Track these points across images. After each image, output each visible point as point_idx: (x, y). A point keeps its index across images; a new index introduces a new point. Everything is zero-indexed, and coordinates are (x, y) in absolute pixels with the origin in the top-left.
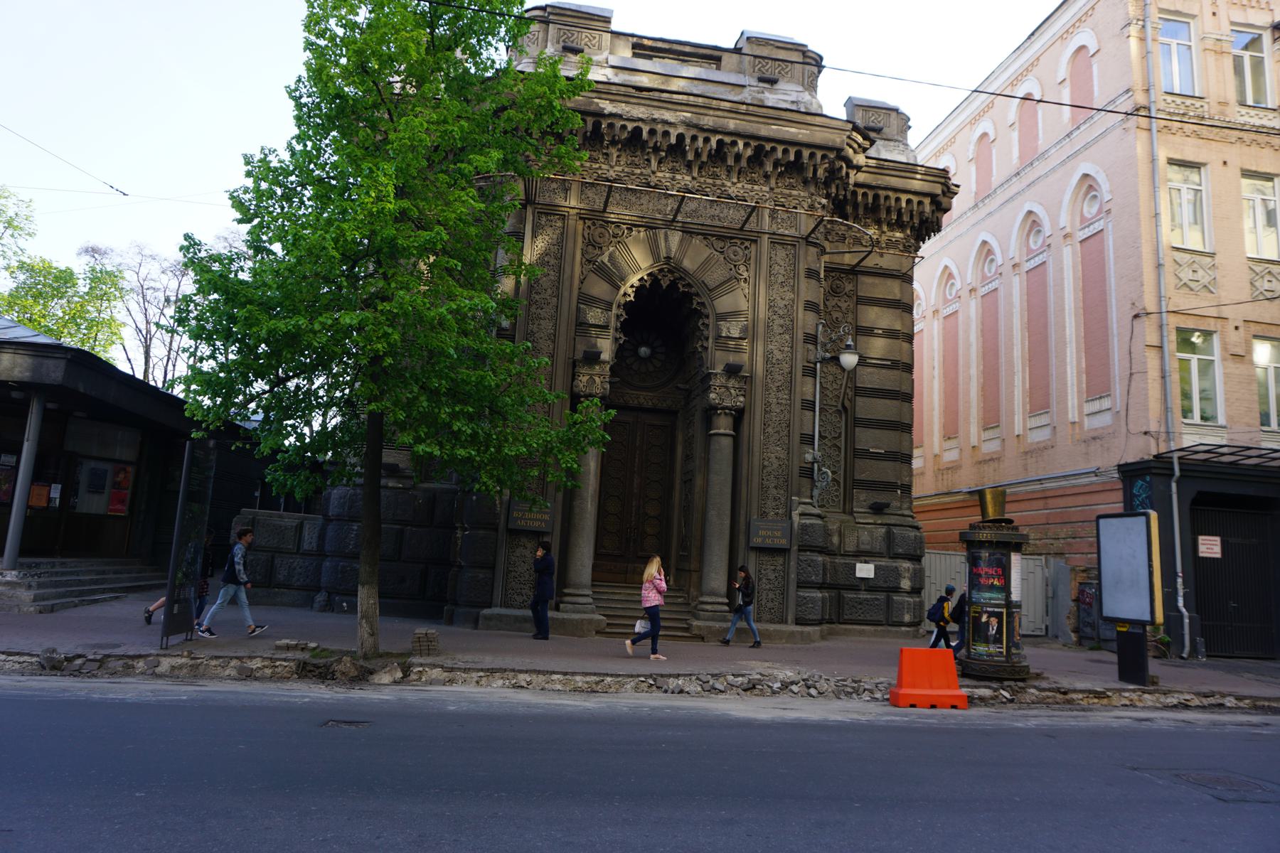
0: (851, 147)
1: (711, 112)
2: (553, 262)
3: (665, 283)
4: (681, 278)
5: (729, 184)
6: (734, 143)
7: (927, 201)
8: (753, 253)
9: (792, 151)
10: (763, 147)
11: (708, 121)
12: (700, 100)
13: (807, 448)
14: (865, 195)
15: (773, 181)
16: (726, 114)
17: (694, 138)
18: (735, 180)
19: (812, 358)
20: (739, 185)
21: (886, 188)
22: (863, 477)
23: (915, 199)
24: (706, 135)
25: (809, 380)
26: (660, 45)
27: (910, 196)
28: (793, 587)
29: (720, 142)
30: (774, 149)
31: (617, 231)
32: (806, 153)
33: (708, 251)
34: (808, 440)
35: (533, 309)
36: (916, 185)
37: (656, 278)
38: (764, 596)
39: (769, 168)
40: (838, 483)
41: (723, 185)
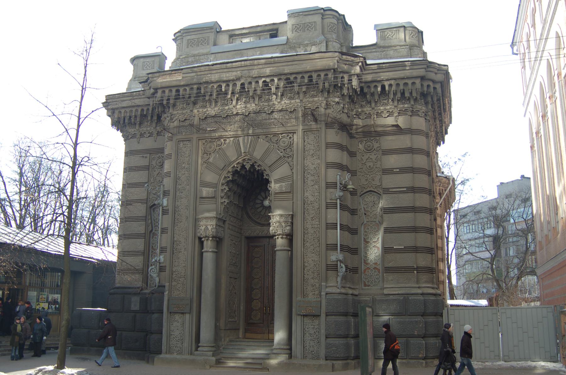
0: (346, 64)
1: (256, 67)
2: (187, 166)
3: (248, 167)
4: (256, 162)
5: (277, 103)
6: (273, 80)
7: (418, 81)
8: (295, 140)
9: (306, 76)
10: (289, 79)
11: (255, 73)
12: (248, 62)
13: (330, 253)
14: (376, 87)
15: (301, 95)
16: (264, 66)
17: (250, 83)
18: (279, 100)
19: (333, 197)
20: (283, 102)
21: (387, 80)
22: (390, 265)
23: (410, 82)
24: (256, 80)
25: (331, 211)
26: (244, 31)
27: (406, 81)
28: (323, 338)
29: (264, 82)
30: (296, 78)
31: (219, 143)
32: (315, 76)
33: (268, 144)
34: (333, 247)
35: (178, 194)
36: (407, 73)
37: (243, 164)
38: (308, 345)
39: (296, 89)
40: (379, 270)
41: (274, 104)
